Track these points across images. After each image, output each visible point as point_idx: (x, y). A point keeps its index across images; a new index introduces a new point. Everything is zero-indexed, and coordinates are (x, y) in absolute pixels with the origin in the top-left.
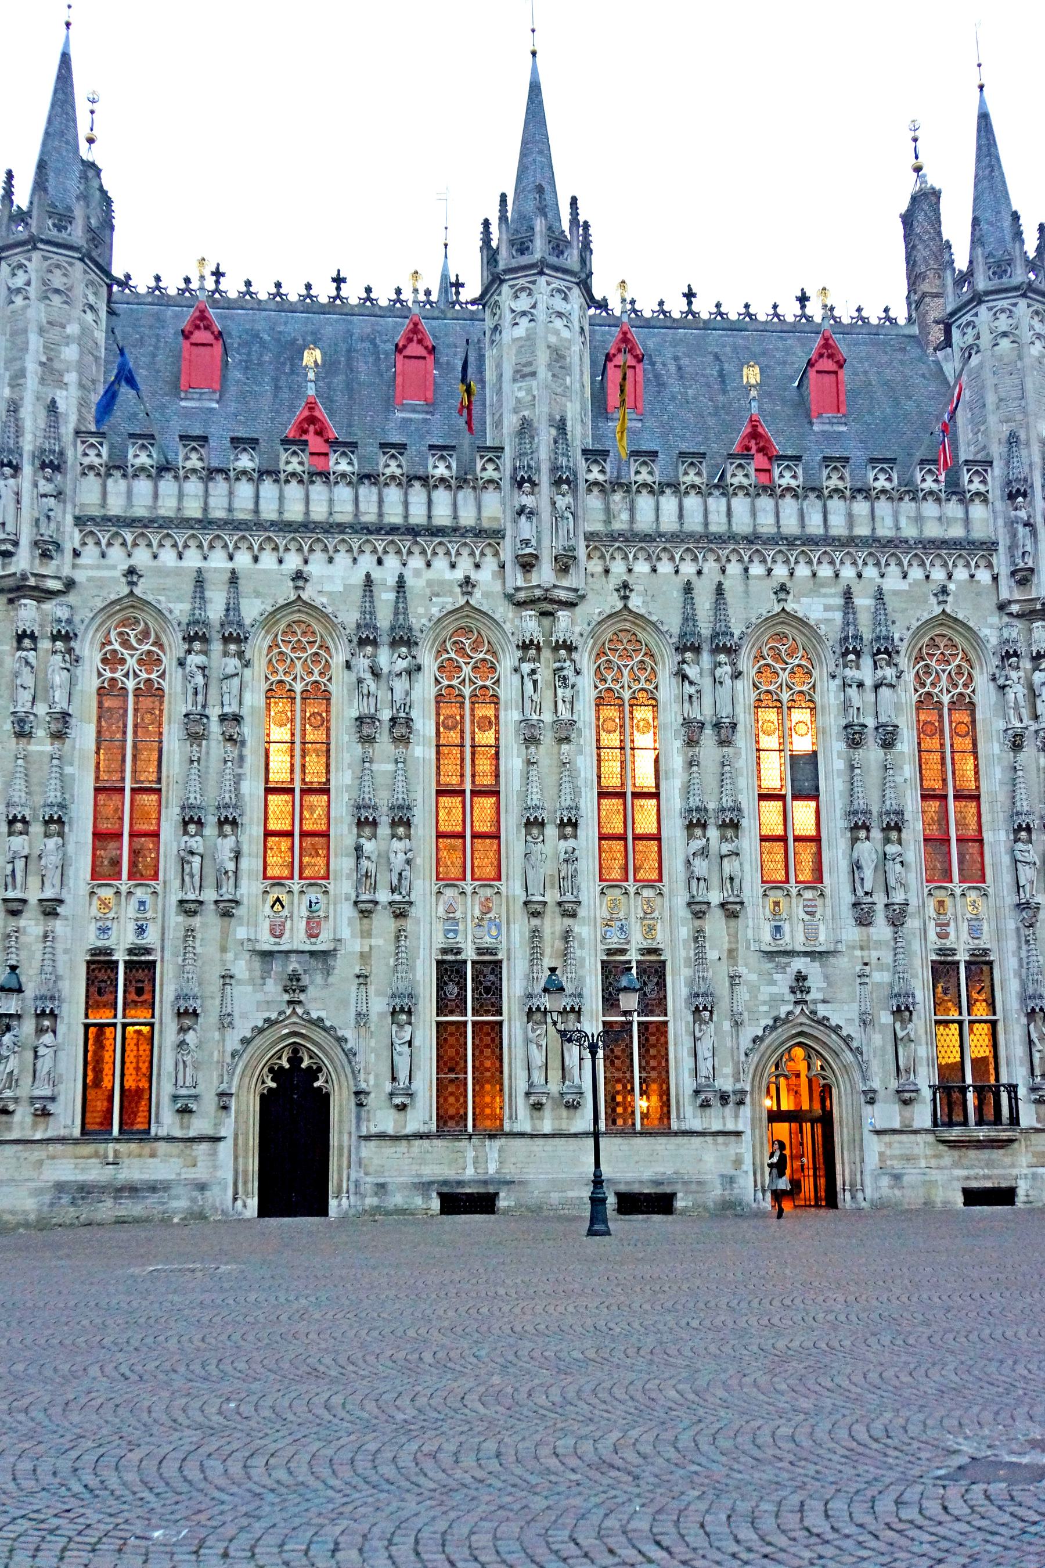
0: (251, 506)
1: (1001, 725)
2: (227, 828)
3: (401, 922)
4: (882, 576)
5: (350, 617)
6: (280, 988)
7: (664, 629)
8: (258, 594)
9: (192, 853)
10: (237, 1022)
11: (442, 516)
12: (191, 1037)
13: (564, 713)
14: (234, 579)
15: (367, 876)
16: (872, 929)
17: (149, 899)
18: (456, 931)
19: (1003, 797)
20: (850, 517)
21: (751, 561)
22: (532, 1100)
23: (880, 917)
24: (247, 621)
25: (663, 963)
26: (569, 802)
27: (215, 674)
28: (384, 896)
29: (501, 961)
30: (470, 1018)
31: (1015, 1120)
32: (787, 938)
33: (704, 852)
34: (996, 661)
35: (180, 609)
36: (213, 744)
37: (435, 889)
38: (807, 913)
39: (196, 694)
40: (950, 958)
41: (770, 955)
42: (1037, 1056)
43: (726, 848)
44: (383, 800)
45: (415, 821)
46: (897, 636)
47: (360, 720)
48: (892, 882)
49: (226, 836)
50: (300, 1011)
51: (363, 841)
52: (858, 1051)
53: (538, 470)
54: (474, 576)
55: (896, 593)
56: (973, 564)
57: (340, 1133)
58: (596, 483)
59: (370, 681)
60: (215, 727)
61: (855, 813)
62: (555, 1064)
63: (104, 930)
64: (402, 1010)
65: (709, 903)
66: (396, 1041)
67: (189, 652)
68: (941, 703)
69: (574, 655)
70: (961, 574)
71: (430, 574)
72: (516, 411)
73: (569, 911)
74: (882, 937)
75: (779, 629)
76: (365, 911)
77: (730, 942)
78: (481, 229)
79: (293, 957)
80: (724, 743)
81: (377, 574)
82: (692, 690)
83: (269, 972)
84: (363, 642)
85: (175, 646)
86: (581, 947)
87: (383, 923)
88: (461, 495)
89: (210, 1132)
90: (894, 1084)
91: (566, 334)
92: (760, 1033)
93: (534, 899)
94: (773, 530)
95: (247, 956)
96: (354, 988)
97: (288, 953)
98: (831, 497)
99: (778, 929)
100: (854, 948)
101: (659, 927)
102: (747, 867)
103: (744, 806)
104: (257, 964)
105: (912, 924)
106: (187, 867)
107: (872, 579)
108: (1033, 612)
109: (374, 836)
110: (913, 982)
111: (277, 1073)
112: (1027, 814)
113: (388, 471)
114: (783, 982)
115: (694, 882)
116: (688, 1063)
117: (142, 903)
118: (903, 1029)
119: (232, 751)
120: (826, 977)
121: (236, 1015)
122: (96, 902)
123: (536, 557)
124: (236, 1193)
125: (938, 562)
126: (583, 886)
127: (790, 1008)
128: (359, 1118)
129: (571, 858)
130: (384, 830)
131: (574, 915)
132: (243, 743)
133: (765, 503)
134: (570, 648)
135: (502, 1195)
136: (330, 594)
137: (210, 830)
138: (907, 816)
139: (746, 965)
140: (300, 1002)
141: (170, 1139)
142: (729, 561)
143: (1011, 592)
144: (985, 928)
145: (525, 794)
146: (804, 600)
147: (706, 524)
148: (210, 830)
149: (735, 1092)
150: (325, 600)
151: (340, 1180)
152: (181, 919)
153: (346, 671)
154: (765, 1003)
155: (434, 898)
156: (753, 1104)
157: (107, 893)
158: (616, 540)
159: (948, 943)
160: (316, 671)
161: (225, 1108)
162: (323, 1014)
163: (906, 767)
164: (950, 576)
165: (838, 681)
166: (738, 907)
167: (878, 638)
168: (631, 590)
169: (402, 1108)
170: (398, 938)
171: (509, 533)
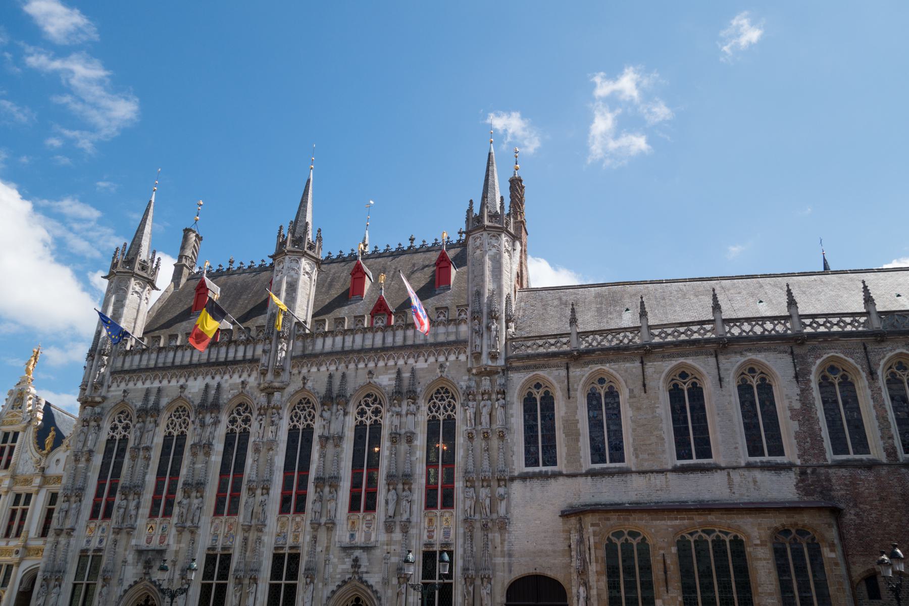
1: (465, 428)
2: (136, 496)
4: (416, 362)
5: (197, 401)
9: (121, 508)
14: (159, 390)
16: (393, 535)
18: (216, 540)
19: (462, 465)
21: (359, 362)
23: (398, 529)
24: (162, 407)
25: (299, 554)
26: (265, 478)
28: (189, 524)
29: (230, 555)
32: (356, 540)
34: (463, 398)
35: (139, 404)
36: (140, 460)
37: (210, 521)
38: (367, 527)
40: (431, 549)
43: (331, 495)
46: (419, 390)
47: (194, 446)
51: (183, 500)
52: (379, 599)
53: (272, 334)
55: (422, 369)
56: (457, 353)
59: (199, 430)
63: (88, 542)
65: (320, 524)
67: (138, 422)
68: (439, 420)
69: (280, 411)
70: (452, 358)
76: (181, 529)
77: (327, 543)
79: (150, 553)
80: (336, 445)
82: (325, 423)
85: (135, 419)
86: (263, 546)
87: (187, 536)
92: (335, 588)
94: (370, 347)
95: (133, 553)
97: (148, 551)
98: (397, 329)
99: (352, 536)
102: (339, 505)
104: (136, 557)
105: (413, 531)
107: (411, 364)
109: (189, 497)
112: (469, 472)
114: (348, 562)
117: (103, 529)
118: (400, 587)
120: (369, 560)
122: (88, 529)
126: (269, 517)
127: (350, 576)
129: (263, 504)
136: (193, 393)
137: (131, 498)
138: (416, 477)
142: (350, 363)
143: (472, 364)
144: (452, 532)
146: (380, 377)
150: (190, 396)
152: (113, 536)
153: (193, 425)
155: (210, 525)
157: (92, 525)
163: (418, 453)
164: (447, 359)
165: (390, 413)
166: (330, 525)
168: (308, 380)
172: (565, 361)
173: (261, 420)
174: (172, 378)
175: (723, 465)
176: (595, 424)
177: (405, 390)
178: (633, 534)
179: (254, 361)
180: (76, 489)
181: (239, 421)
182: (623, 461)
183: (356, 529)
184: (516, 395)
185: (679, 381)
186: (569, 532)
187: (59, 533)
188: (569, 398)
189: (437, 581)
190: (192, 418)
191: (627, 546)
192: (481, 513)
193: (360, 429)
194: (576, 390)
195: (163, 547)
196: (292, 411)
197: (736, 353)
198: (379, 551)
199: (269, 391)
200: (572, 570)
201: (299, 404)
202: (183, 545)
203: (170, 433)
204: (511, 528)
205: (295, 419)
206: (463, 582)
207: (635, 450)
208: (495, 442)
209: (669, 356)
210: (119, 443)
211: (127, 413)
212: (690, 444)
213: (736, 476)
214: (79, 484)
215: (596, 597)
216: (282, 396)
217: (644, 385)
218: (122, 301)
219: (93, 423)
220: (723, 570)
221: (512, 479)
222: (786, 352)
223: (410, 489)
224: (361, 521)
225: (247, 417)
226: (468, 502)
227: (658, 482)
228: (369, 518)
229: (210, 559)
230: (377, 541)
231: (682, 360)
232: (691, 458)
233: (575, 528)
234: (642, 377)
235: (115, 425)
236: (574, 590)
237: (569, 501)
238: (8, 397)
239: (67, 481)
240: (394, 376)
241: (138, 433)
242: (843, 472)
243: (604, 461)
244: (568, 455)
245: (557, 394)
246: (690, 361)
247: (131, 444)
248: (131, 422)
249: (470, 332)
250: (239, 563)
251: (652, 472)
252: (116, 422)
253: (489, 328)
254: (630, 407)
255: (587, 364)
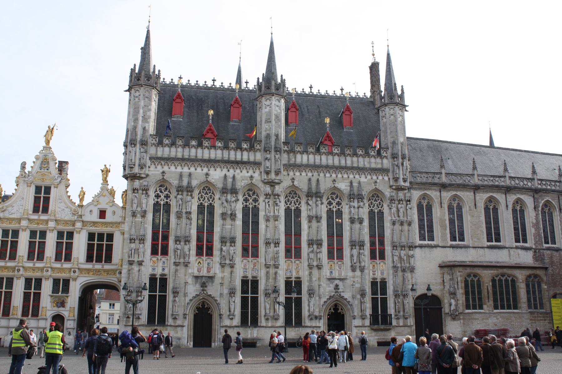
0: (195, 155)
1: (390, 218)
2: (187, 243)
3: (232, 269)
5: (220, 185)
6: (200, 286)
7: (303, 190)
8: (196, 179)
9: (178, 249)
10: (189, 295)
11: (245, 158)
12: (177, 299)
13: (277, 213)
14: (190, 175)
15: (224, 256)
16: (356, 273)
17: (166, 261)
18: (246, 272)
20: (352, 162)
21: (326, 173)
22: (266, 317)
23: (358, 270)
24: (193, 186)
25: (301, 281)
26: (277, 238)
27: (184, 200)
28: (228, 262)
29: (258, 280)
30: (250, 295)
31: (391, 324)
32: (334, 275)
33: (312, 252)
35: (175, 182)
37: (241, 260)
39: (180, 206)
41: (329, 279)
42: (397, 307)
43: (318, 251)
44: (228, 235)
45: (236, 242)
46: (364, 194)
48: (361, 260)
49: (186, 245)
50: (205, 292)
51: (223, 247)
52: (351, 305)
53: (271, 148)
54: (253, 175)
55: (364, 182)
57: (215, 325)
58: (286, 151)
59: (225, 204)
60: (184, 215)
61: (352, 242)
62: (272, 308)
63: (154, 269)
64: (232, 293)
66: (231, 301)
67: (178, 194)
68: (375, 212)
69: (279, 197)
70: (380, 178)
71: (241, 174)
72: (265, 131)
73: (276, 267)
75: (333, 191)
76: (223, 266)
78: (257, 80)
79: (204, 278)
81: (228, 174)
82: (310, 207)
83: (197, 282)
84: (223, 193)
85: (174, 193)
87: (228, 270)
88: (250, 153)
89: (182, 324)
90: (360, 314)
91: (279, 111)
92: (326, 300)
93: (268, 263)
95: (191, 277)
96: (219, 287)
97: (202, 277)
99: (331, 272)
100: (351, 278)
101: (300, 271)
102: (324, 256)
103: (323, 239)
104: (194, 280)
105: (366, 271)
106: (176, 253)
108: (399, 188)
111: (198, 308)
113: (231, 146)
115: (310, 260)
116: (307, 308)
117: (164, 262)
118: (363, 299)
119: (188, 222)
120: (344, 286)
121: (188, 293)
122: (152, 261)
123: (270, 171)
124: (188, 341)
125: (375, 174)
126: (281, 260)
127: (334, 293)
128: (220, 321)
129: (277, 253)
130: (228, 244)
131: (278, 268)
132: (191, 219)
133: (330, 157)
134: (278, 195)
135: (258, 342)
136: (215, 179)
137: (182, 243)
138: (366, 242)
139: (323, 282)
140: (205, 290)
141: (171, 326)
144: (385, 272)
145: (266, 235)
146: (340, 184)
147: (315, 162)
148: (182, 243)
149: (319, 316)
150: (213, 181)
151: (215, 338)
152: (174, 267)
154: (327, 292)
156: (324, 319)
157: (155, 259)
158: (291, 166)
159: (375, 276)
160: (211, 200)
161: (185, 318)
162: (211, 293)
164: (378, 178)
165: (348, 206)
167: (359, 195)
169: (232, 319)
170: (231, 273)
171: (263, 164)
172: (438, 188)
173: (269, 202)
174: (197, 167)
175: (507, 246)
176: (452, 222)
177: (356, 193)
178: (475, 276)
179: (257, 164)
180: (142, 236)
181: (251, 201)
182: (464, 241)
184: (415, 203)
185: (488, 204)
186: (443, 274)
187: (131, 263)
188: (441, 207)
189: (379, 296)
190: (217, 196)
191: (472, 281)
192: (401, 263)
193: (330, 213)
194: (444, 204)
195: (211, 274)
196: (285, 198)
197: (513, 194)
199: (272, 184)
200: (445, 292)
201: (289, 194)
202: (225, 274)
203: (201, 203)
204: (416, 271)
205: (289, 203)
206: (394, 297)
207: (471, 236)
208: (406, 227)
209: (486, 192)
210: (163, 206)
211: (165, 187)
212: (492, 235)
213: (512, 251)
214: (142, 233)
215: (461, 304)
216: (279, 188)
217: (475, 205)
218: (148, 106)
219: (140, 192)
220: (507, 293)
221: (416, 247)
222: (531, 196)
223: (363, 249)
225: (255, 198)
226: (396, 258)
227: (481, 252)
228: (340, 263)
229: (244, 282)
230: (347, 276)
231: (491, 194)
232: (493, 242)
233: (447, 273)
234: (474, 201)
235: (158, 194)
236: (446, 301)
237: (443, 259)
238: (35, 160)
239: (130, 229)
240: (349, 184)
241: (181, 202)
242: (549, 252)
243: (456, 241)
244: (442, 236)
245: (435, 204)
246: (495, 195)
247: (174, 209)
248: (170, 193)
249: (391, 164)
250: (266, 285)
251: (478, 248)
252: (159, 192)
253: (402, 164)
254: (470, 215)
255: (450, 190)
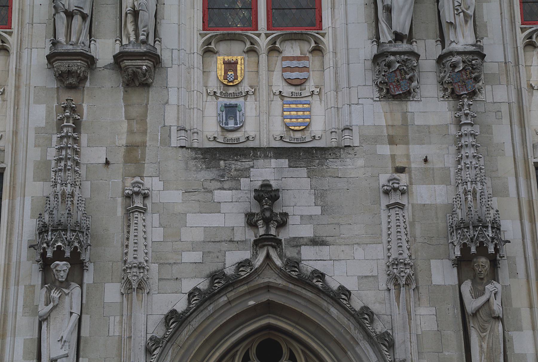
16: (411, 106)
38: (289, 82)
65: (91, 61)
74: (433, 121)
77: (131, 132)
92: (181, 306)
100: (376, 140)
110: (495, 202)
118: (477, 293)
127: (246, 255)
166: (145, 65)
183: (245, 87)
198: (360, 162)
224: (263, 58)
